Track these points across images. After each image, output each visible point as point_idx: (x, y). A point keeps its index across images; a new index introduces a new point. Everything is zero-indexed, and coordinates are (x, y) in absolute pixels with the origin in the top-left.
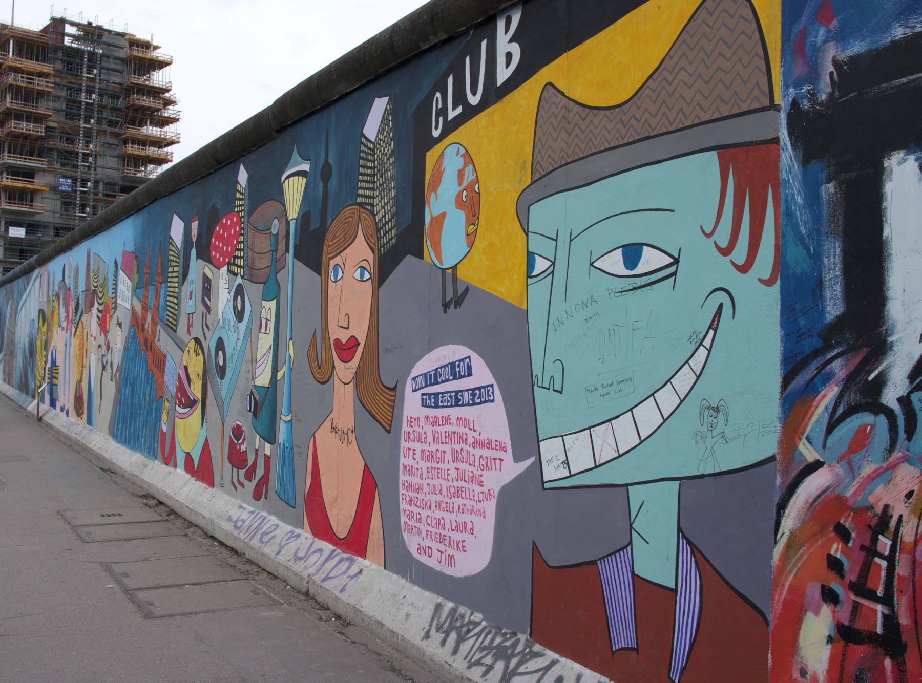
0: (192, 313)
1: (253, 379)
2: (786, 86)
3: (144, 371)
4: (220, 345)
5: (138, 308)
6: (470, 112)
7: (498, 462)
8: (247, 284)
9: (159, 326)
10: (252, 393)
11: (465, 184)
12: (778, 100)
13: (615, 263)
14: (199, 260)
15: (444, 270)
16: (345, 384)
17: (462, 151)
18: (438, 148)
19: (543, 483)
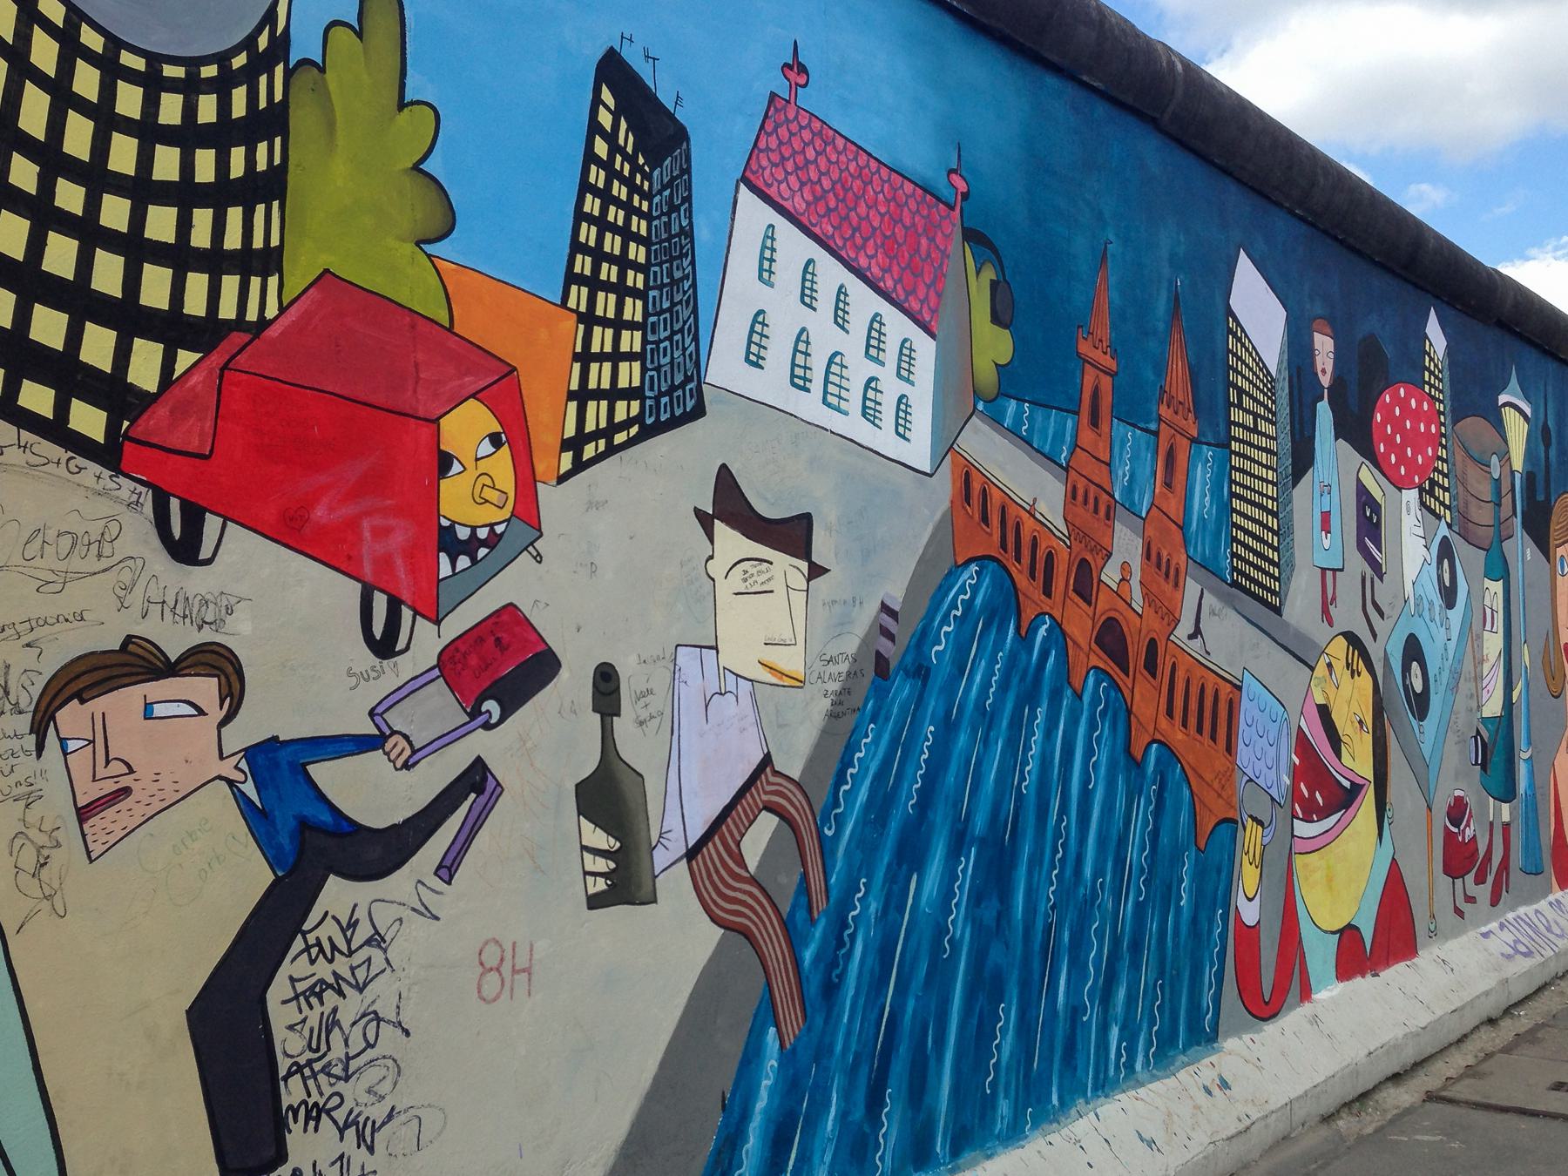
0: (1334, 570)
1: (1479, 707)
3: (1102, 756)
4: (1413, 652)
8: (1458, 543)
9: (1192, 588)
10: (1478, 732)
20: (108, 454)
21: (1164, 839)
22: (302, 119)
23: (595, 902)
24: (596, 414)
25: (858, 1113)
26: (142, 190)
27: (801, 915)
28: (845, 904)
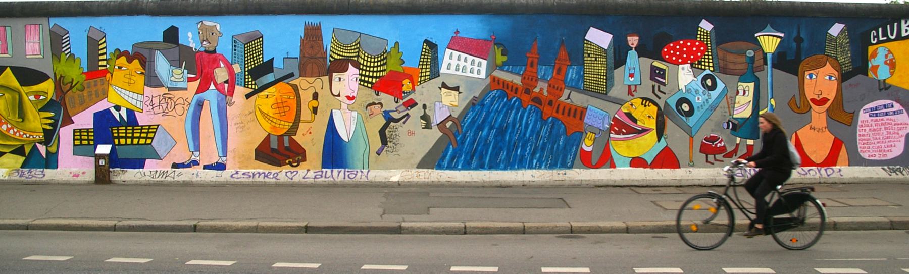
0: (636, 86)
6: (889, 40)
11: (888, 58)
14: (641, 58)
15: (879, 81)
16: (819, 113)
18: (875, 47)
20: (371, 88)
21: (554, 132)
22: (388, 57)
23: (423, 128)
24: (422, 79)
25: (468, 158)
26: (374, 67)
27: (457, 134)
28: (466, 132)
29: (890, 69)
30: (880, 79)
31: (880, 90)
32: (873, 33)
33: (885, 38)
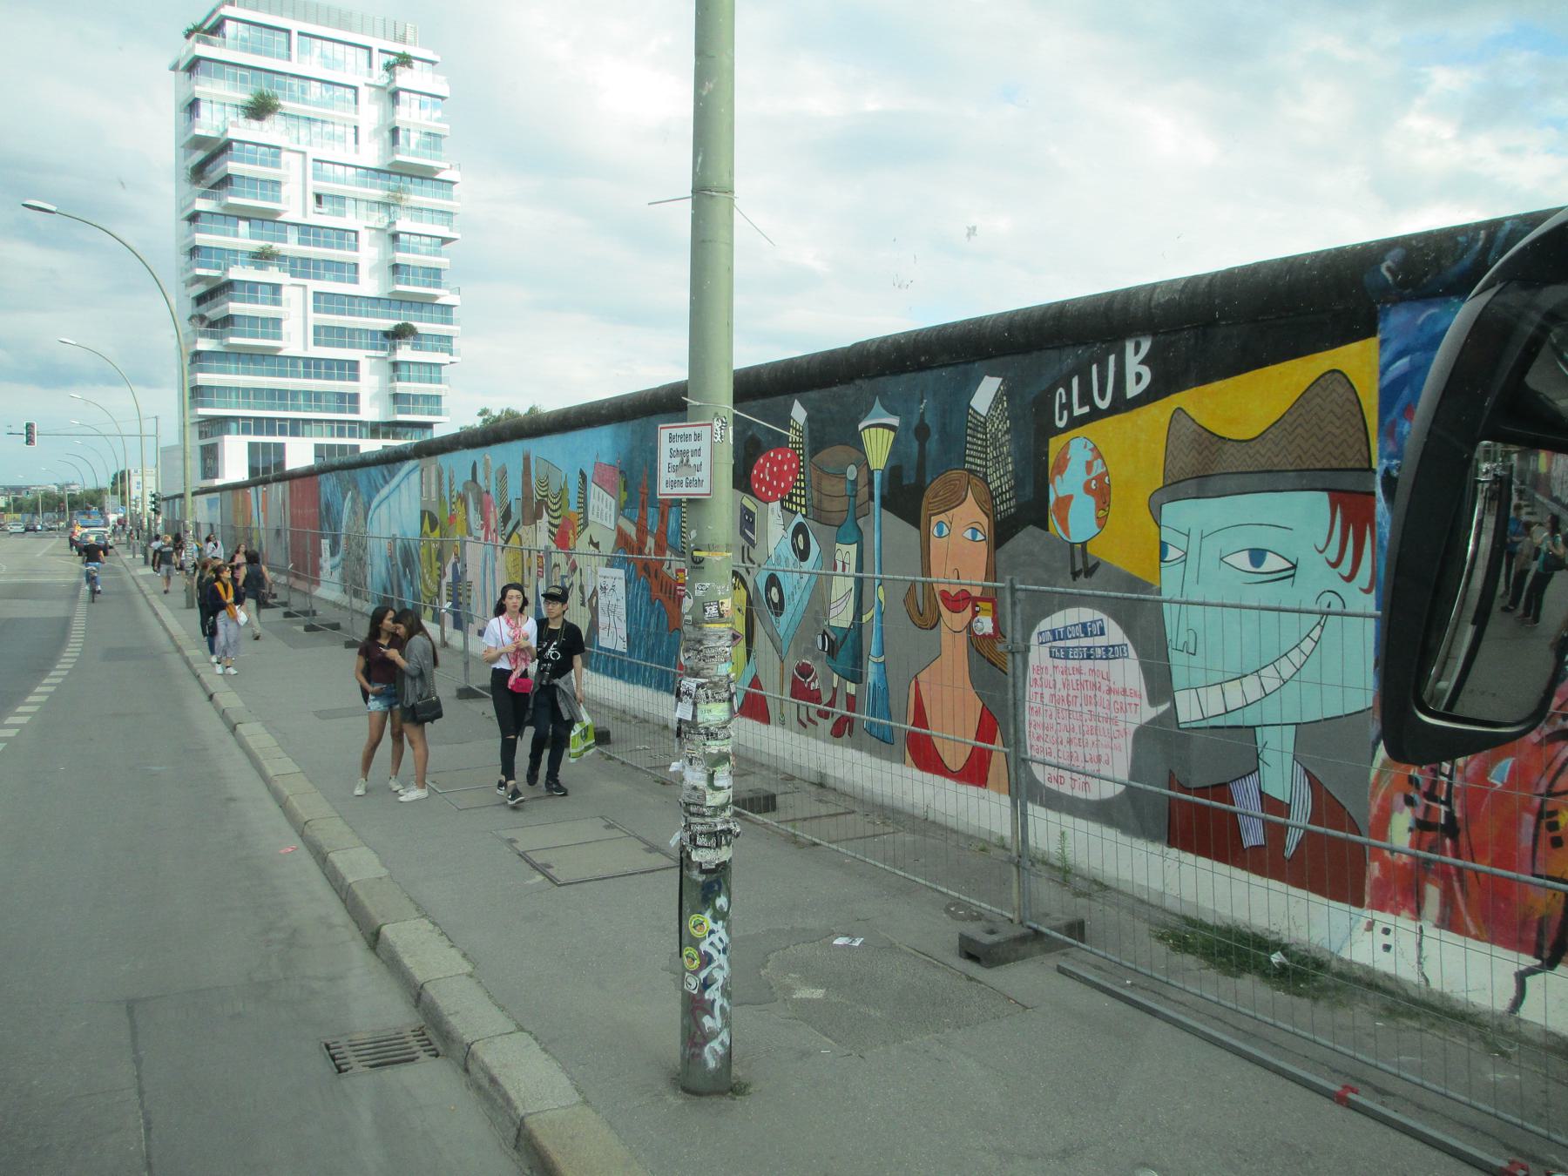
2: (1381, 457)
3: (645, 599)
4: (773, 581)
5: (631, 530)
6: (1096, 414)
7: (1133, 706)
8: (811, 525)
11: (1094, 474)
12: (1375, 465)
13: (1243, 561)
15: (1072, 544)
17: (1090, 446)
18: (1063, 438)
19: (1178, 724)
29: (1098, 508)
30: (1072, 541)
31: (1075, 575)
32: (1060, 394)
33: (1086, 409)
